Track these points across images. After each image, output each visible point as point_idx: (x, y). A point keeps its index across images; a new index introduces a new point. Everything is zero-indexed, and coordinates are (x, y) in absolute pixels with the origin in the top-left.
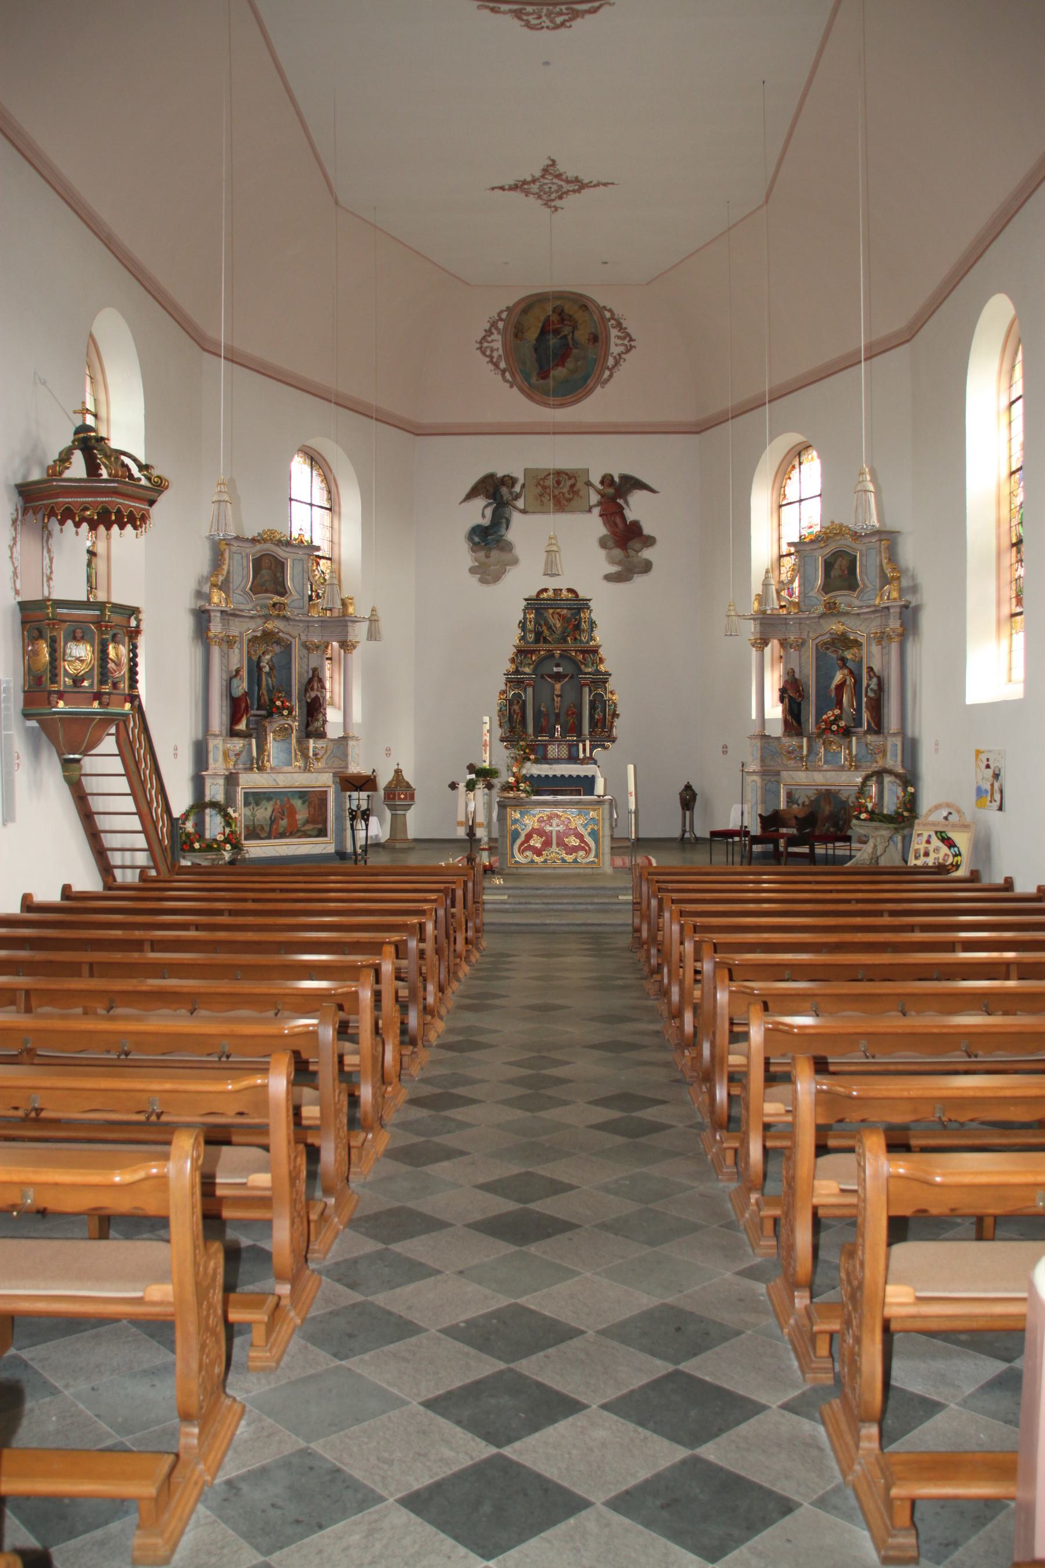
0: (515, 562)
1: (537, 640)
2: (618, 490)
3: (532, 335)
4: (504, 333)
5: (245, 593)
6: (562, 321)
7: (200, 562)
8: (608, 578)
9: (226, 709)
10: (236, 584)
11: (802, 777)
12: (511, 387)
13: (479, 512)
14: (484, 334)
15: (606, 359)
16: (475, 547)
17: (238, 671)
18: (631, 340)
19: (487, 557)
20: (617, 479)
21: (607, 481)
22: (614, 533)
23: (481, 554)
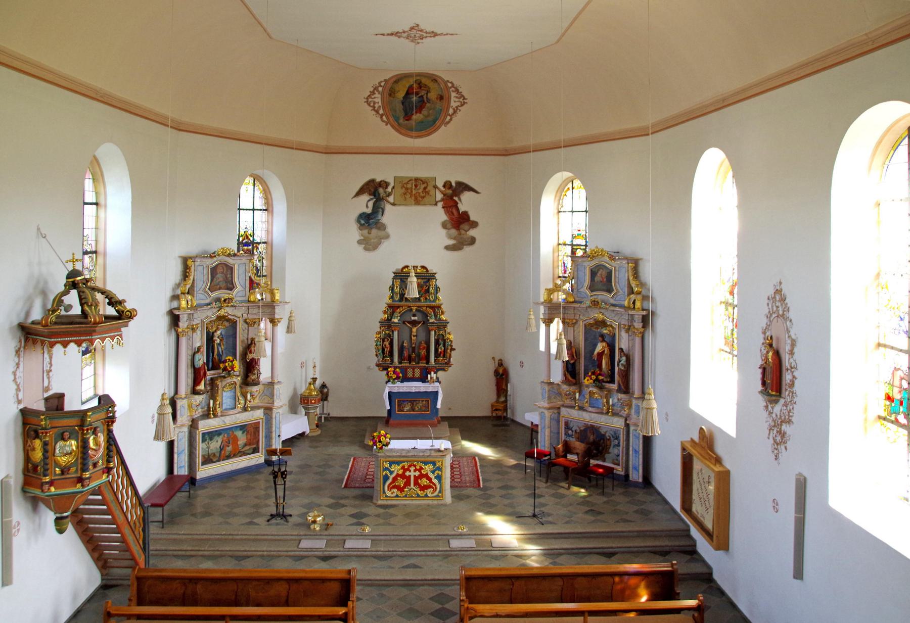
0: (387, 237)
1: (401, 299)
2: (455, 190)
3: (401, 95)
4: (382, 94)
5: (206, 292)
7: (174, 272)
8: (447, 248)
9: (191, 376)
10: (199, 286)
11: (574, 414)
13: (364, 204)
15: (448, 109)
16: (361, 227)
17: (199, 348)
19: (369, 233)
20: (454, 184)
21: (447, 186)
22: (452, 219)
23: (365, 232)
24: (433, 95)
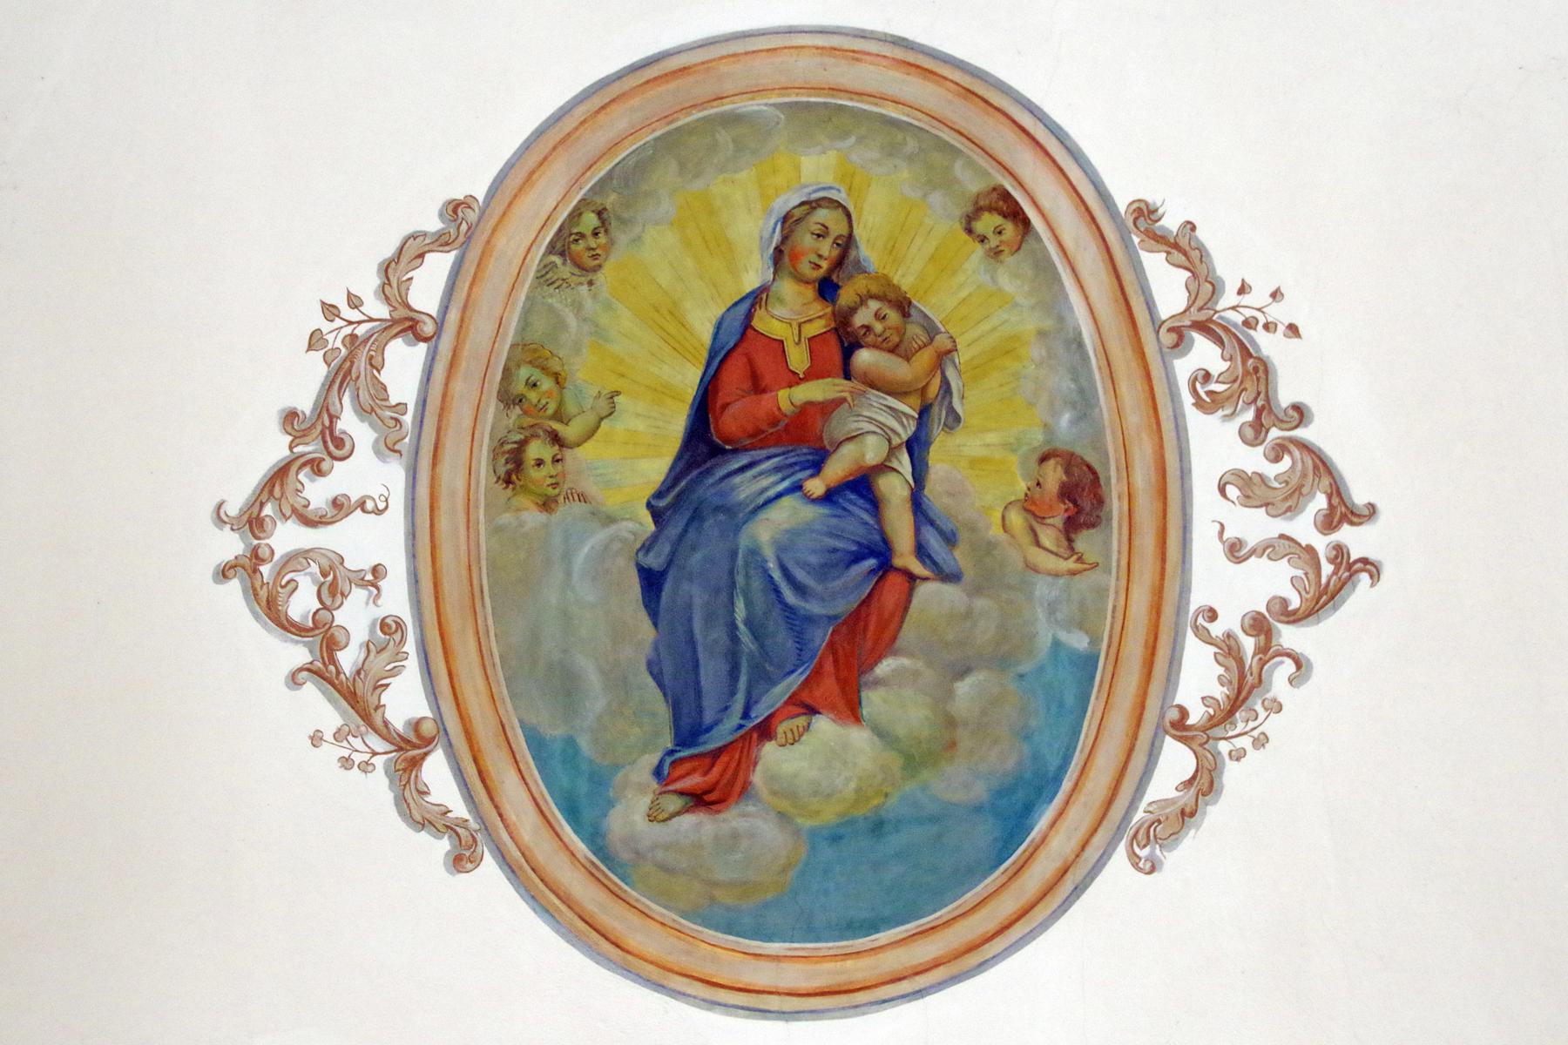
3: (631, 457)
4: (419, 443)
6: (844, 342)
12: (461, 861)
14: (278, 447)
15: (1159, 661)
18: (1342, 512)
24: (982, 470)
